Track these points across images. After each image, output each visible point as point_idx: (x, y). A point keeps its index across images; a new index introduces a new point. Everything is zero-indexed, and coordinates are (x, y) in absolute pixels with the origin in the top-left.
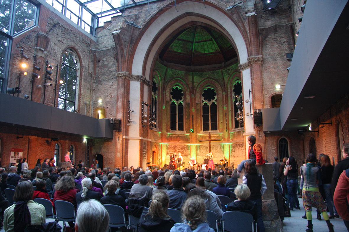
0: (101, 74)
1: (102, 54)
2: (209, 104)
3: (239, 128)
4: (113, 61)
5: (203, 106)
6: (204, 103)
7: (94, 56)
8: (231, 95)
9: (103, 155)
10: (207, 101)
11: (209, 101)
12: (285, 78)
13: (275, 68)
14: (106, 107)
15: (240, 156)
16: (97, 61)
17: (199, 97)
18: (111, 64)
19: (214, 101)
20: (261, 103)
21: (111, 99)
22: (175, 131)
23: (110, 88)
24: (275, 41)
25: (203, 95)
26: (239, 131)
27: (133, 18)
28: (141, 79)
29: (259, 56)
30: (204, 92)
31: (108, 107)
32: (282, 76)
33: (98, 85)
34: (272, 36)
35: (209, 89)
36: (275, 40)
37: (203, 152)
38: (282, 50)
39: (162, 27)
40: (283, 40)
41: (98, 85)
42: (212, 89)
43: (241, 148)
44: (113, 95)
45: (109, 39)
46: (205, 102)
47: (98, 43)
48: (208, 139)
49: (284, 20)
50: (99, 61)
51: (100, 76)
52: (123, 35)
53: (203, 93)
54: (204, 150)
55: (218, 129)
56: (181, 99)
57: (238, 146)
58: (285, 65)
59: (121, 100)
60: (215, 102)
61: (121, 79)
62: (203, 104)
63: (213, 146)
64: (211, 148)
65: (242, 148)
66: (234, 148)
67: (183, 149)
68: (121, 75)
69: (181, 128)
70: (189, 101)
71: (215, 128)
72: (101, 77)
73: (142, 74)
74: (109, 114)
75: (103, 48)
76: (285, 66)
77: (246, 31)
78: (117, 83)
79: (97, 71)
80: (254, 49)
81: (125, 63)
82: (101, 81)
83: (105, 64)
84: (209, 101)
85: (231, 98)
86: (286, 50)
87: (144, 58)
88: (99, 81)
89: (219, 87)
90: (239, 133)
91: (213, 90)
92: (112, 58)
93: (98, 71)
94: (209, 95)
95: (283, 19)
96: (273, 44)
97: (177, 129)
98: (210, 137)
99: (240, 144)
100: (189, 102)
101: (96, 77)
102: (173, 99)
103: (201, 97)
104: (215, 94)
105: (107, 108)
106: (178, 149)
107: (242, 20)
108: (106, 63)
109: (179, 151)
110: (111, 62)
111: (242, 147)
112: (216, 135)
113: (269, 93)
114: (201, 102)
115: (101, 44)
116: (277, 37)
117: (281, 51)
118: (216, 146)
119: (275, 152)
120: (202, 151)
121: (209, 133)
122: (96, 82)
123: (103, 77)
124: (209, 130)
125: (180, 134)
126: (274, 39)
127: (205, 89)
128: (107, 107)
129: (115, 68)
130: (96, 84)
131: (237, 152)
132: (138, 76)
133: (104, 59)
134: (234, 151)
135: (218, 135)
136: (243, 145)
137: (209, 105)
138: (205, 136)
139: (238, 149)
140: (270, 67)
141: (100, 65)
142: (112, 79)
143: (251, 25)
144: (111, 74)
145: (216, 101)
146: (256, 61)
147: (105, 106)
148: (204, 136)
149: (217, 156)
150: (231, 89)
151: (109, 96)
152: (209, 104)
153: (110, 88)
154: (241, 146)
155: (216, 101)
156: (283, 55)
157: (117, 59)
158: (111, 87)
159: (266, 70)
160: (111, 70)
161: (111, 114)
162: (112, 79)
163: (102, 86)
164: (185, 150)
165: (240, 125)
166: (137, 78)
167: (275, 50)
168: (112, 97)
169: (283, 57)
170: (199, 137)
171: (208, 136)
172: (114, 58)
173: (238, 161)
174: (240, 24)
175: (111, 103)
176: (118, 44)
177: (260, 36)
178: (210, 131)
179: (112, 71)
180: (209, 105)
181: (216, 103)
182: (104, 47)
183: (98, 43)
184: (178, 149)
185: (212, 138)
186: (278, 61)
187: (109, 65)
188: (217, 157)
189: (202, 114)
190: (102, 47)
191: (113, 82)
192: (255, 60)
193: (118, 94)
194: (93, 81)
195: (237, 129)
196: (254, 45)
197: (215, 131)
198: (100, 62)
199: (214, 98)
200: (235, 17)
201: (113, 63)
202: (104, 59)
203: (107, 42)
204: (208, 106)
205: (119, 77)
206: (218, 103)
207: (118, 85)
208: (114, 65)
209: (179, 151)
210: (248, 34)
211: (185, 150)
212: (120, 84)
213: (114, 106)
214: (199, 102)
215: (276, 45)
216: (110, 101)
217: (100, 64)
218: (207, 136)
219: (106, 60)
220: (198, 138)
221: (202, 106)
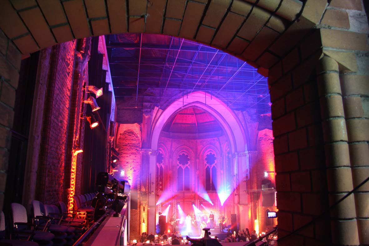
6: (179, 166)
10: (181, 165)
19: (187, 165)
25: (178, 159)
30: (179, 156)
42: (187, 154)
46: (180, 165)
56: (162, 162)
60: (188, 166)
62: (178, 167)
91: (187, 156)
104: (189, 160)
127: (180, 154)
137: (184, 169)
145: (189, 165)
155: (189, 165)
165: (211, 188)
176: (146, 124)
199: (187, 163)
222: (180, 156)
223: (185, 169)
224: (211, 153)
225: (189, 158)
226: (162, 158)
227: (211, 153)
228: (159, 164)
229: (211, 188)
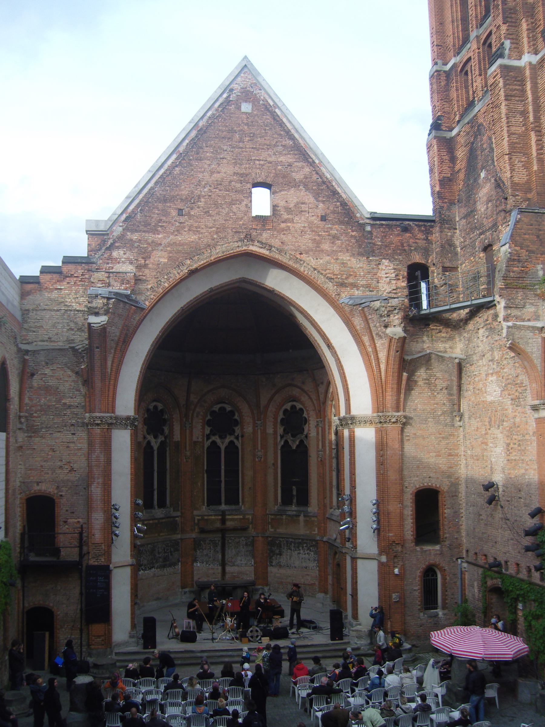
0: (39, 408)
1: (43, 359)
2: (223, 445)
3: (294, 508)
4: (71, 379)
5: (208, 448)
7: (24, 363)
8: (275, 433)
9: (53, 610)
11: (222, 437)
12: (440, 458)
13: (424, 438)
14: (57, 493)
15: (295, 567)
16: (29, 375)
17: (199, 426)
18: (67, 385)
20: (399, 506)
21: (69, 475)
22: (153, 511)
23: (68, 447)
24: (425, 385)
25: (209, 423)
26: (294, 513)
27: (128, 282)
28: (132, 424)
29: (399, 414)
31: (63, 494)
32: (435, 454)
33: (31, 437)
34: (421, 374)
35: (222, 409)
36: (427, 383)
37: (207, 555)
38: (437, 404)
39: (185, 303)
40: (441, 384)
41: (31, 437)
42: (230, 409)
43: (299, 550)
44: (75, 466)
45: (57, 319)
47: (26, 326)
48: (218, 525)
49: (443, 345)
50: (33, 375)
51: (35, 415)
52: (111, 327)
53: (209, 417)
54: (210, 549)
55: (241, 504)
57: (291, 544)
58: (441, 434)
59: (100, 480)
60: (235, 441)
61: (97, 431)
62: (207, 444)
63: (230, 541)
64: (226, 546)
65: (302, 552)
66: (281, 547)
67: (167, 550)
68: (99, 422)
69: (162, 504)
70: (179, 436)
71: (233, 499)
72: (39, 417)
73: (135, 411)
74: (67, 510)
75: (44, 341)
76: (441, 436)
77: (377, 359)
78: (86, 437)
79: (27, 400)
80: (390, 398)
81: (108, 390)
82: (42, 428)
83: (50, 386)
84: (222, 437)
85: (275, 438)
86: (444, 404)
87: (141, 372)
88: (33, 426)
89: (246, 410)
90: (295, 518)
91: (232, 413)
92: (70, 373)
93: (31, 399)
94: (223, 422)
95: (442, 341)
96: (424, 390)
97: (156, 507)
98: (223, 521)
99: (297, 541)
100: (179, 440)
101: (26, 417)
102: (149, 433)
103: (203, 428)
104: (236, 423)
105: (61, 495)
106: (159, 553)
107: (374, 335)
108: (52, 382)
109: (160, 555)
110: (67, 381)
111: (301, 548)
112: (236, 517)
113: (412, 485)
114: (203, 440)
115: (34, 330)
116: (431, 376)
117: (436, 405)
118: (237, 540)
119: (417, 594)
120: (205, 552)
121: (223, 514)
122: (24, 427)
123: (44, 417)
124: (220, 504)
125: (162, 516)
126: (425, 379)
127: (214, 409)
128: (61, 493)
129: (79, 400)
130: (26, 434)
131: (288, 557)
132: (128, 418)
133: (47, 371)
134: (277, 555)
135: (241, 517)
136: (305, 545)
138: (213, 517)
139: (289, 551)
140: (415, 434)
141: (35, 384)
142: (73, 425)
143: (392, 353)
144: (68, 412)
146: (394, 422)
147: (56, 492)
148: (210, 517)
149: (238, 562)
150: (275, 418)
151: (66, 467)
152: (223, 445)
153: (68, 447)
154: (298, 547)
156: (439, 414)
157: (88, 382)
158: (71, 445)
159: (409, 440)
160: (67, 401)
161: (73, 513)
162: (73, 425)
163: (44, 441)
164: (171, 552)
165: (295, 501)
166: (126, 422)
167: (426, 402)
168: (72, 470)
169: (439, 417)
170: (199, 520)
171: (220, 517)
172: (77, 373)
173: (290, 577)
174: (366, 339)
175: (70, 484)
176: (97, 348)
177: (405, 374)
178: (223, 507)
179: (70, 407)
180: (223, 448)
181: (238, 444)
182: (45, 339)
183: (26, 326)
184: (159, 553)
185: (229, 524)
186: (429, 424)
187: (61, 388)
188: (238, 566)
189: (205, 468)
190: (41, 339)
191: (74, 434)
192: (392, 421)
193: (90, 466)
194: (19, 426)
195: (288, 508)
196: (392, 391)
197: (233, 507)
198: (35, 376)
200: (358, 322)
201: (73, 384)
202: (47, 371)
203: (54, 326)
204: (219, 448)
205: (92, 425)
206: (242, 445)
207: (91, 444)
208: (77, 390)
209: (160, 555)
210: (383, 367)
211: (171, 552)
212: (97, 441)
213: (81, 493)
214: (200, 440)
215: (427, 393)
216: (68, 480)
217: (36, 382)
218: (217, 517)
219: (51, 374)
220: (196, 521)
221: (205, 449)
222: (213, 413)
223: (226, 448)
224: (293, 407)
225: (236, 417)
226: (165, 421)
227: (293, 407)
228: (156, 437)
229: (295, 501)
